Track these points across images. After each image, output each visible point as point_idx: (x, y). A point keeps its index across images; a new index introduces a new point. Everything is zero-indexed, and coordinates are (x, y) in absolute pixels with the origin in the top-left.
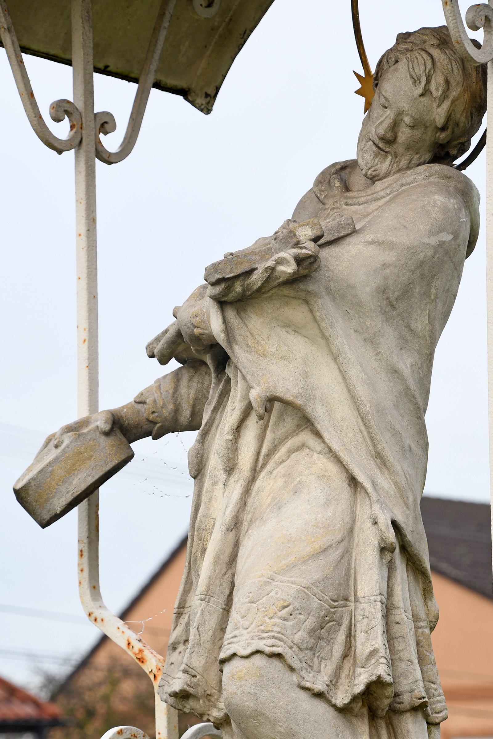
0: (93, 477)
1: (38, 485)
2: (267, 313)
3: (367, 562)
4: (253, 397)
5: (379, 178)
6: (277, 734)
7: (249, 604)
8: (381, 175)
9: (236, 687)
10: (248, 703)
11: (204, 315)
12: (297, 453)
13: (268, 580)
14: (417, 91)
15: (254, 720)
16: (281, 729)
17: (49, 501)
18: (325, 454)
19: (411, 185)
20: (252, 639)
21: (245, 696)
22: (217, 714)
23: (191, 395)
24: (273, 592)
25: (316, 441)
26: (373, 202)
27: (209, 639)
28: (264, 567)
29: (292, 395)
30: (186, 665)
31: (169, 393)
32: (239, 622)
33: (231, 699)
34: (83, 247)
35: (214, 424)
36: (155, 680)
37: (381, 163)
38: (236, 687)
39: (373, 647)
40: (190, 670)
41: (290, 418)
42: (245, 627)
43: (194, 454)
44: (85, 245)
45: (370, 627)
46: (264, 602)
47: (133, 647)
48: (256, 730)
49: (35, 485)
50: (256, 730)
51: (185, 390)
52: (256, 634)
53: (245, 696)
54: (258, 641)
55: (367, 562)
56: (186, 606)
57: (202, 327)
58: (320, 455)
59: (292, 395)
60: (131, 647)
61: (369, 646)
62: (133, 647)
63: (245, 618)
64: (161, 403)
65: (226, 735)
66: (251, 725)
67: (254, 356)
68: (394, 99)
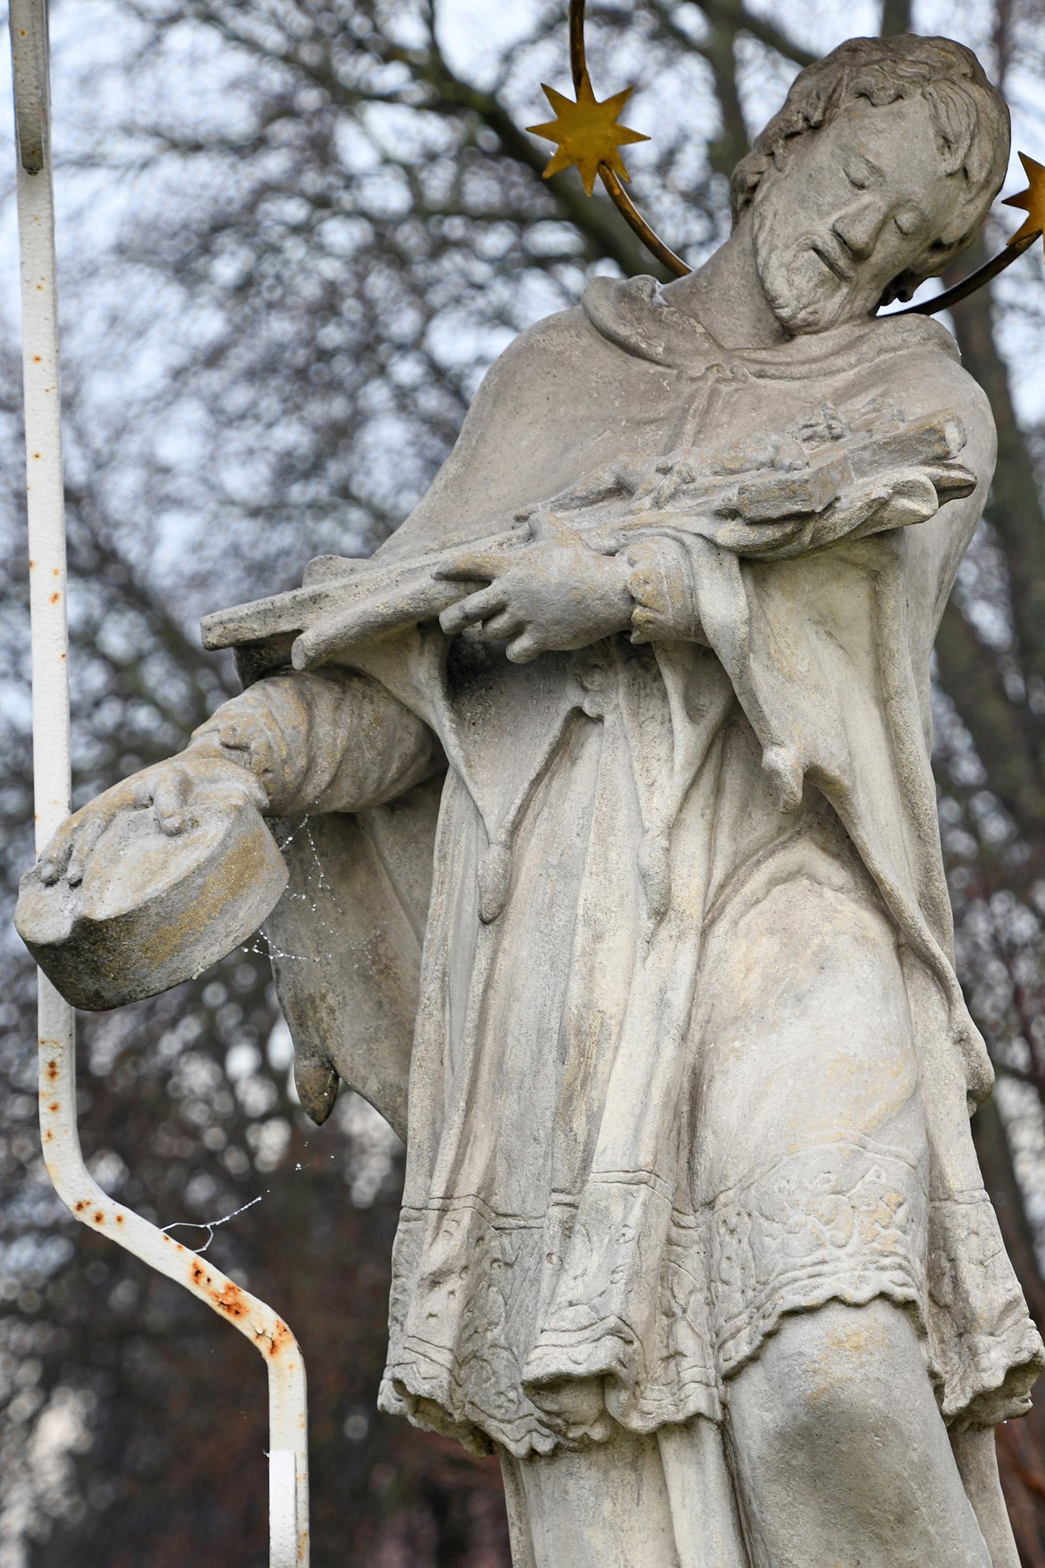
0: (268, 904)
1: (167, 913)
2: (803, 590)
3: (950, 1121)
4: (789, 764)
5: (816, 328)
6: (906, 1466)
7: (833, 1196)
8: (822, 324)
9: (851, 1366)
10: (873, 1401)
11: (661, 582)
12: (783, 886)
13: (857, 1148)
14: (944, 164)
15: (877, 1436)
16: (914, 1456)
17: (183, 950)
18: (849, 891)
19: (899, 353)
20: (866, 1269)
21: (870, 1385)
22: (641, 1424)
23: (339, 741)
24: (871, 1173)
25: (830, 865)
26: (821, 378)
27: (654, 1266)
28: (835, 1121)
29: (839, 767)
30: (620, 1318)
31: (299, 732)
32: (822, 1232)
33: (840, 1390)
34: (48, 387)
35: (530, 811)
36: (272, 1352)
37: (827, 298)
38: (851, 1366)
39: (1012, 1294)
40: (626, 1329)
41: (760, 812)
42: (840, 1242)
43: (500, 870)
44: (54, 384)
45: (989, 1254)
46: (862, 1192)
47: (209, 1280)
48: (872, 1456)
49: (158, 914)
50: (872, 1456)
51: (328, 728)
52: (869, 1258)
53: (870, 1385)
54: (877, 1272)
55: (950, 1121)
56: (456, 1195)
57: (655, 606)
58: (840, 895)
59: (839, 767)
60: (205, 1280)
61: (1002, 1292)
62: (209, 1280)
63: (833, 1224)
64: (285, 753)
65: (589, 1468)
66: (867, 1445)
67: (776, 678)
68: (896, 175)
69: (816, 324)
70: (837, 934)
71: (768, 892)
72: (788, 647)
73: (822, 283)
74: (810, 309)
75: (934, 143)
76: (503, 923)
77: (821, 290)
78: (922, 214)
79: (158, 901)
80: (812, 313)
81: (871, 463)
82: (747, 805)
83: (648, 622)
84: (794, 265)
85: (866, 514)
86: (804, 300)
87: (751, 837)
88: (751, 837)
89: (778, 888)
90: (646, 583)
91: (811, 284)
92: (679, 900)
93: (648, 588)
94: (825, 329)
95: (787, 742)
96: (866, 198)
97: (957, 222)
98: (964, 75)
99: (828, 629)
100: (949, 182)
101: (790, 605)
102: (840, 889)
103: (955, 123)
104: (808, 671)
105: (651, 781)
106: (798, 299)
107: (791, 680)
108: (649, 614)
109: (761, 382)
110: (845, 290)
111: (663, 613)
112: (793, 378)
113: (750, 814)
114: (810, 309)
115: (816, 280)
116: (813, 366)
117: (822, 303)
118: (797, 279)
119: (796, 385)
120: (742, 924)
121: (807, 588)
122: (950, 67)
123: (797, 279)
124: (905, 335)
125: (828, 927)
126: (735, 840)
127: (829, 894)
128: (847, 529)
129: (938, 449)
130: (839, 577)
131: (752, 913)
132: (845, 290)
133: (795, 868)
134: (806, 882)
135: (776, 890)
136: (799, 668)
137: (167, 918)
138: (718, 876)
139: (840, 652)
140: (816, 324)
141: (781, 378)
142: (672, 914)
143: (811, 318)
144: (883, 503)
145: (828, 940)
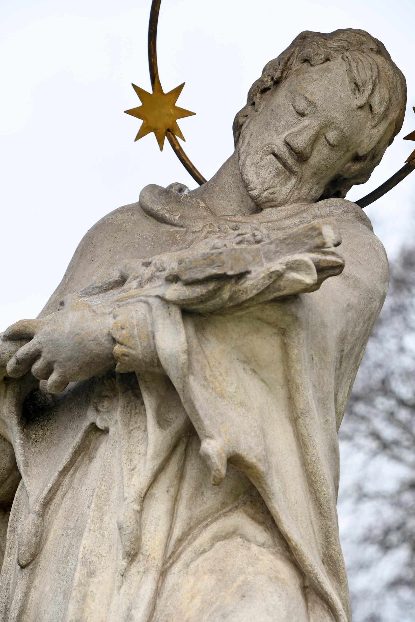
69: (275, 201)
70: (257, 574)
71: (212, 545)
72: (221, 375)
73: (278, 175)
74: (271, 191)
75: (349, 87)
76: (35, 567)
77: (278, 180)
78: (342, 132)
80: (271, 193)
81: (275, 253)
82: (200, 486)
83: (124, 355)
85: (268, 282)
86: (266, 185)
87: (202, 508)
88: (202, 508)
89: (220, 543)
90: (123, 328)
91: (271, 175)
92: (147, 547)
93: (124, 332)
94: (281, 205)
95: (216, 435)
96: (306, 121)
97: (367, 140)
98: (372, 49)
99: (252, 367)
100: (360, 113)
101: (222, 347)
102: (262, 545)
103: (362, 75)
104: (236, 392)
105: (132, 467)
106: (262, 184)
107: (222, 396)
108: (124, 350)
110: (294, 181)
111: (134, 349)
113: (203, 493)
114: (271, 191)
115: (274, 173)
116: (270, 224)
117: (278, 188)
118: (262, 172)
120: (192, 566)
121: (235, 336)
122: (362, 44)
123: (262, 172)
124: (332, 208)
125: (251, 569)
126: (190, 509)
127: (254, 548)
128: (255, 292)
129: (318, 241)
130: (258, 331)
131: (200, 559)
132: (294, 181)
133: (232, 529)
134: (239, 540)
135: (218, 545)
136: (229, 389)
138: (177, 533)
139: (263, 384)
140: (275, 201)
142: (140, 557)
143: (271, 197)
144: (279, 275)
145: (250, 578)
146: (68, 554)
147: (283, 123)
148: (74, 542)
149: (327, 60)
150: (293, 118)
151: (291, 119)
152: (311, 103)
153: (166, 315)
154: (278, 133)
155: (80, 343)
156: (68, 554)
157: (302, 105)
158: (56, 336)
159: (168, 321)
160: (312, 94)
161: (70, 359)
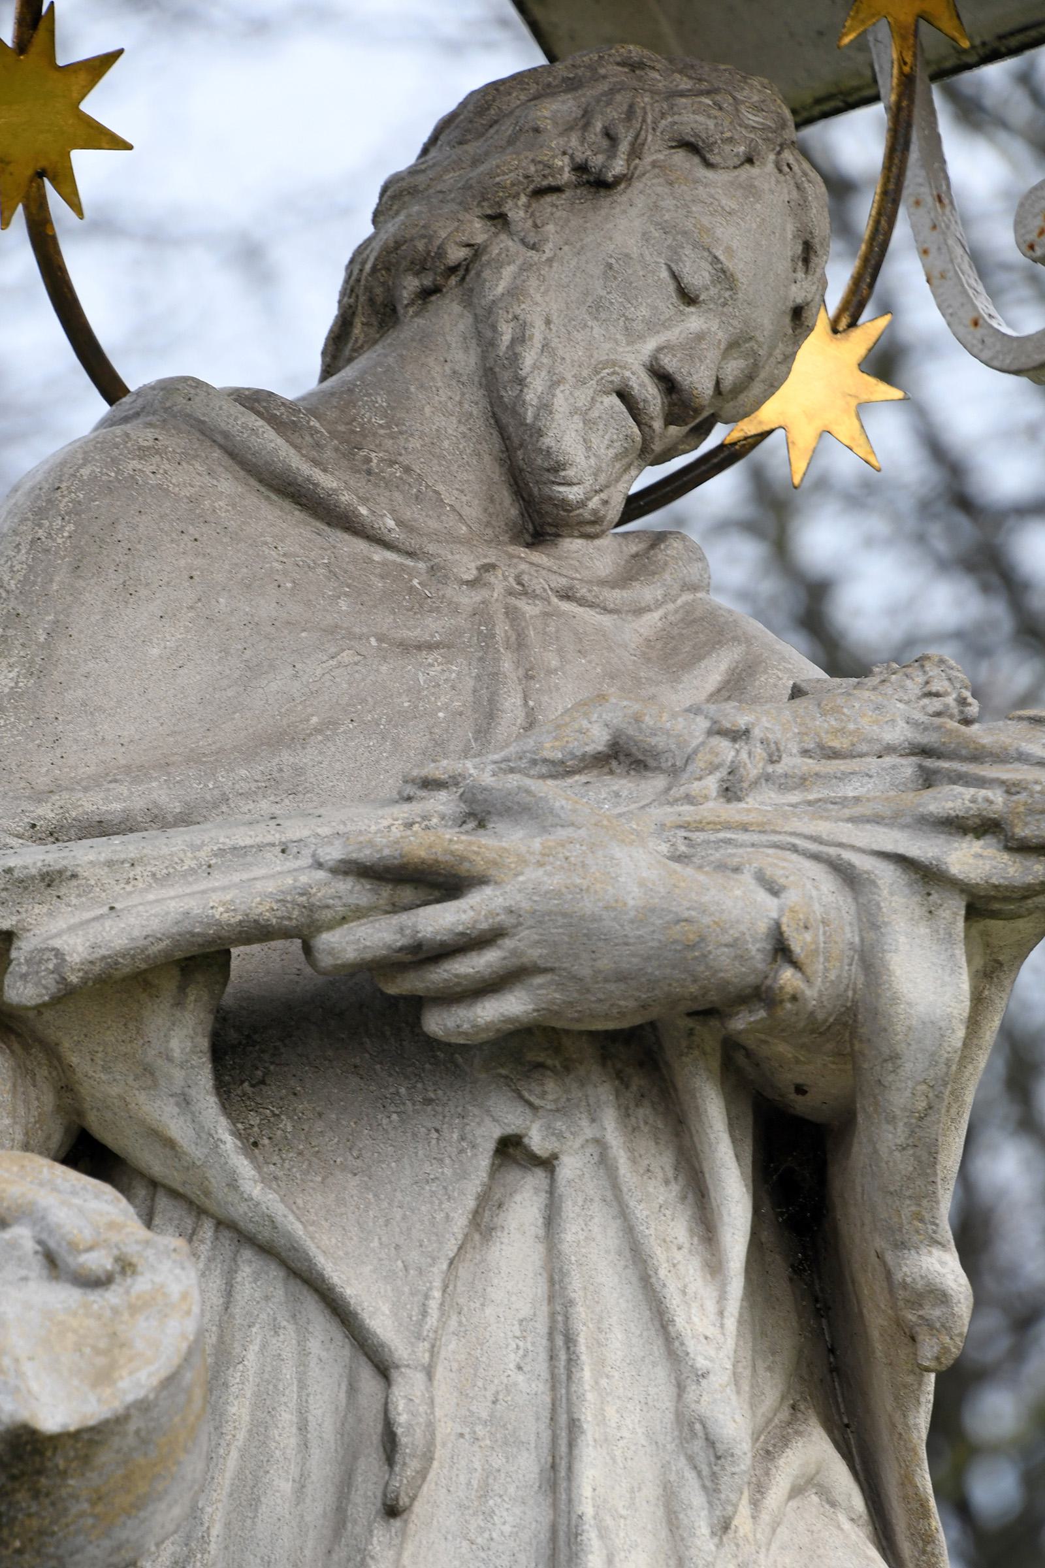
79: (143, 1406)
84: (594, 414)
96: (694, 321)
109: (566, 606)
112: (606, 610)
115: (618, 447)
119: (606, 620)
137: (144, 1440)
141: (592, 605)
146: (485, 1492)
147: (644, 311)
148: (497, 1461)
149: (750, 161)
150: (665, 300)
151: (662, 306)
152: (724, 277)
153: (919, 912)
154: (633, 337)
155: (691, 947)
156: (485, 1492)
157: (697, 275)
158: (588, 906)
159: (923, 930)
160: (729, 250)
161: (621, 977)
